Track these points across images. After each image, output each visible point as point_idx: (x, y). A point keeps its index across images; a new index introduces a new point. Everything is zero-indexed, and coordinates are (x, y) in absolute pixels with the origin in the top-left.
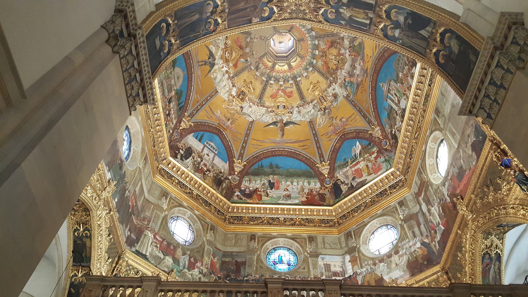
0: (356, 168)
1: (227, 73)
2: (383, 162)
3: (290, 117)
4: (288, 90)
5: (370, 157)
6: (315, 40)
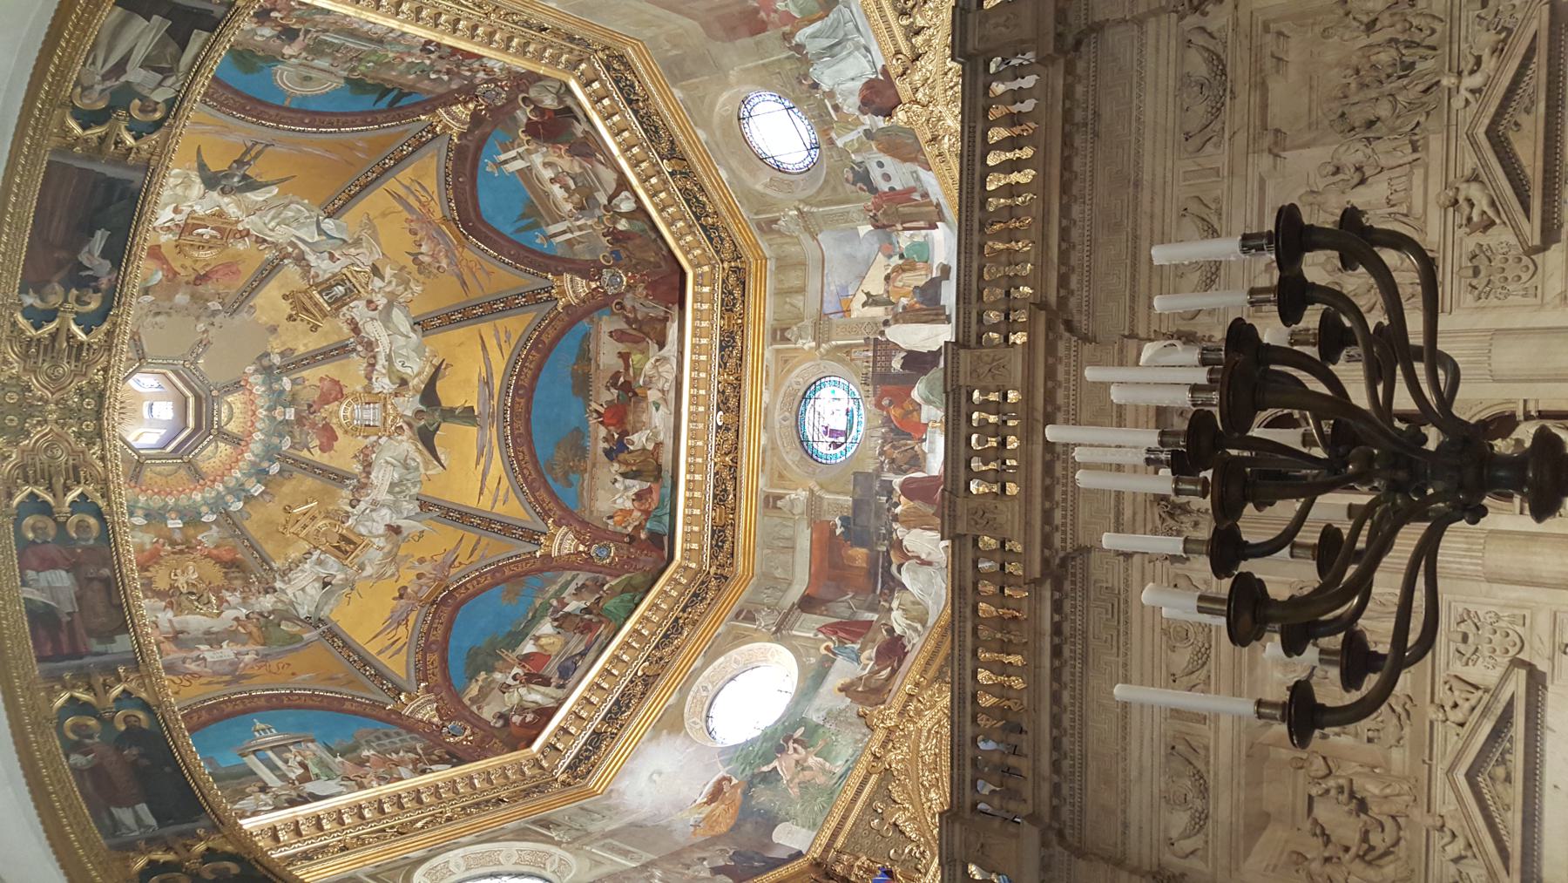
6: (214, 513)
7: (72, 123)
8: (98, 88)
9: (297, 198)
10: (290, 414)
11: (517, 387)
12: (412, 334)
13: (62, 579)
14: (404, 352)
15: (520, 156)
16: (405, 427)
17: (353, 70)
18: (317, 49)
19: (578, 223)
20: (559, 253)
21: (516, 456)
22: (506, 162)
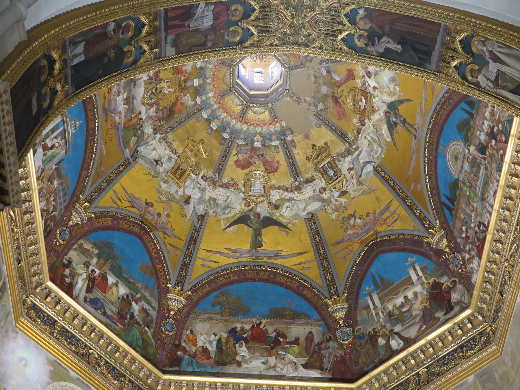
1: (369, 72)
6: (201, 102)
7: (463, 35)
8: (485, 49)
9: (384, 151)
10: (258, 145)
11: (275, 274)
12: (306, 212)
13: (208, 22)
14: (295, 208)
15: (419, 278)
16: (250, 208)
17: (464, 183)
18: (475, 164)
19: (380, 313)
20: (361, 301)
21: (231, 272)
22: (415, 269)
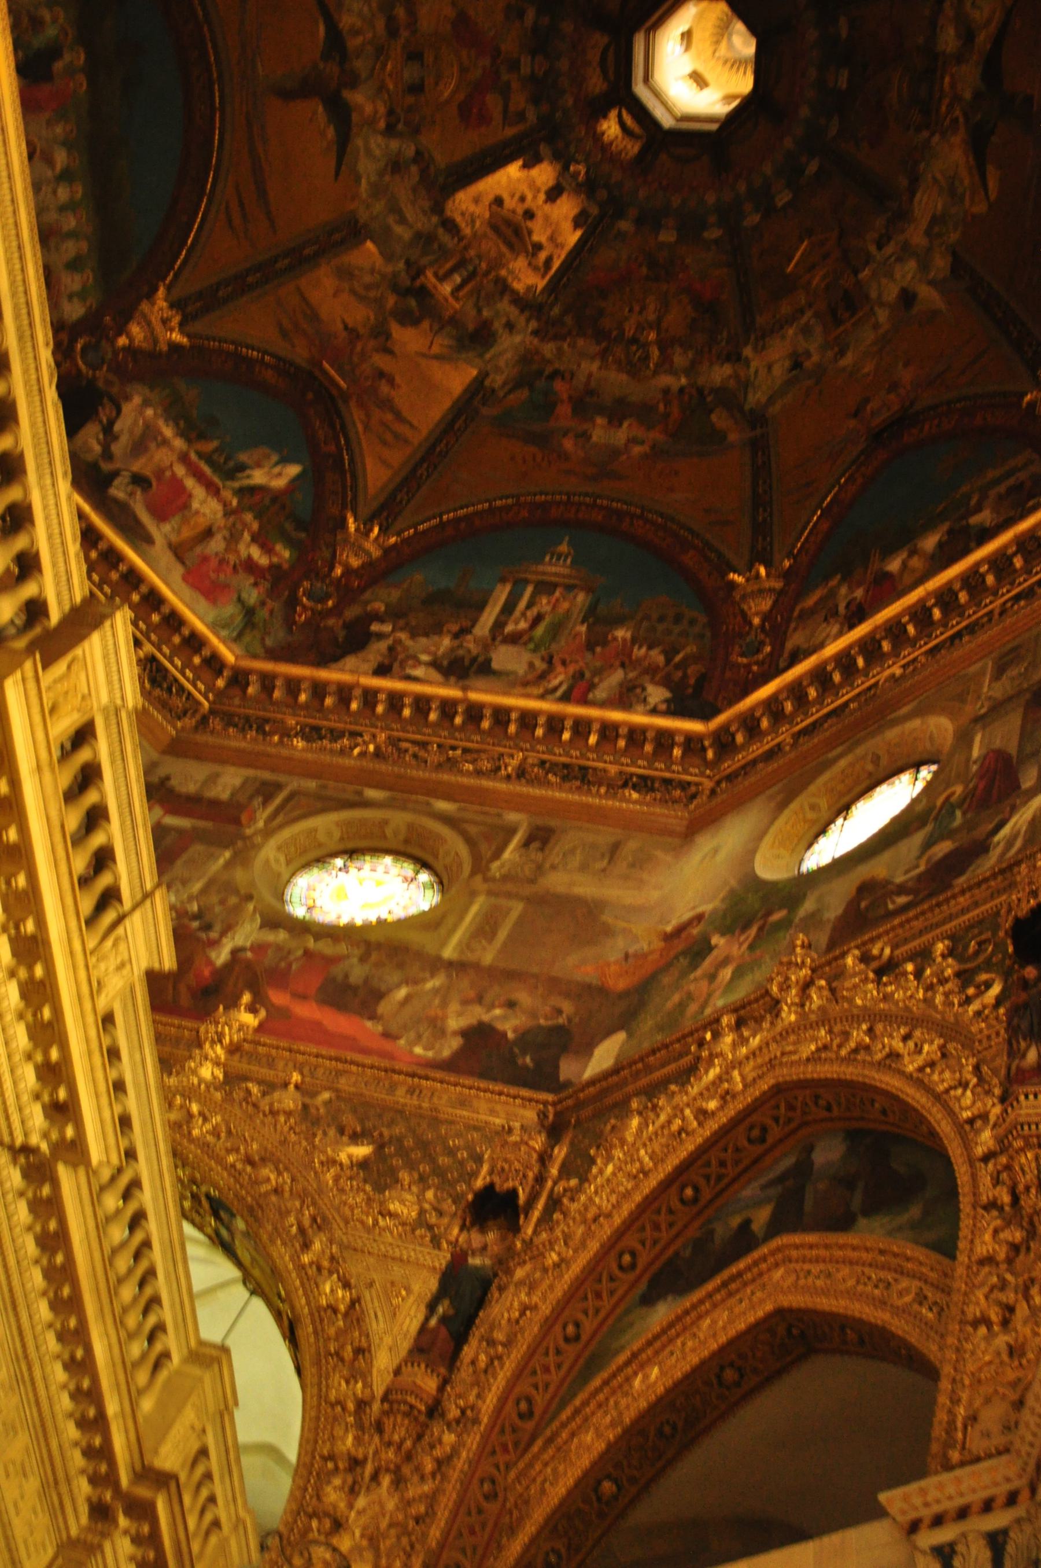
0: (190, 483)
2: (239, 600)
3: (372, 122)
4: (493, 102)
5: (247, 536)
